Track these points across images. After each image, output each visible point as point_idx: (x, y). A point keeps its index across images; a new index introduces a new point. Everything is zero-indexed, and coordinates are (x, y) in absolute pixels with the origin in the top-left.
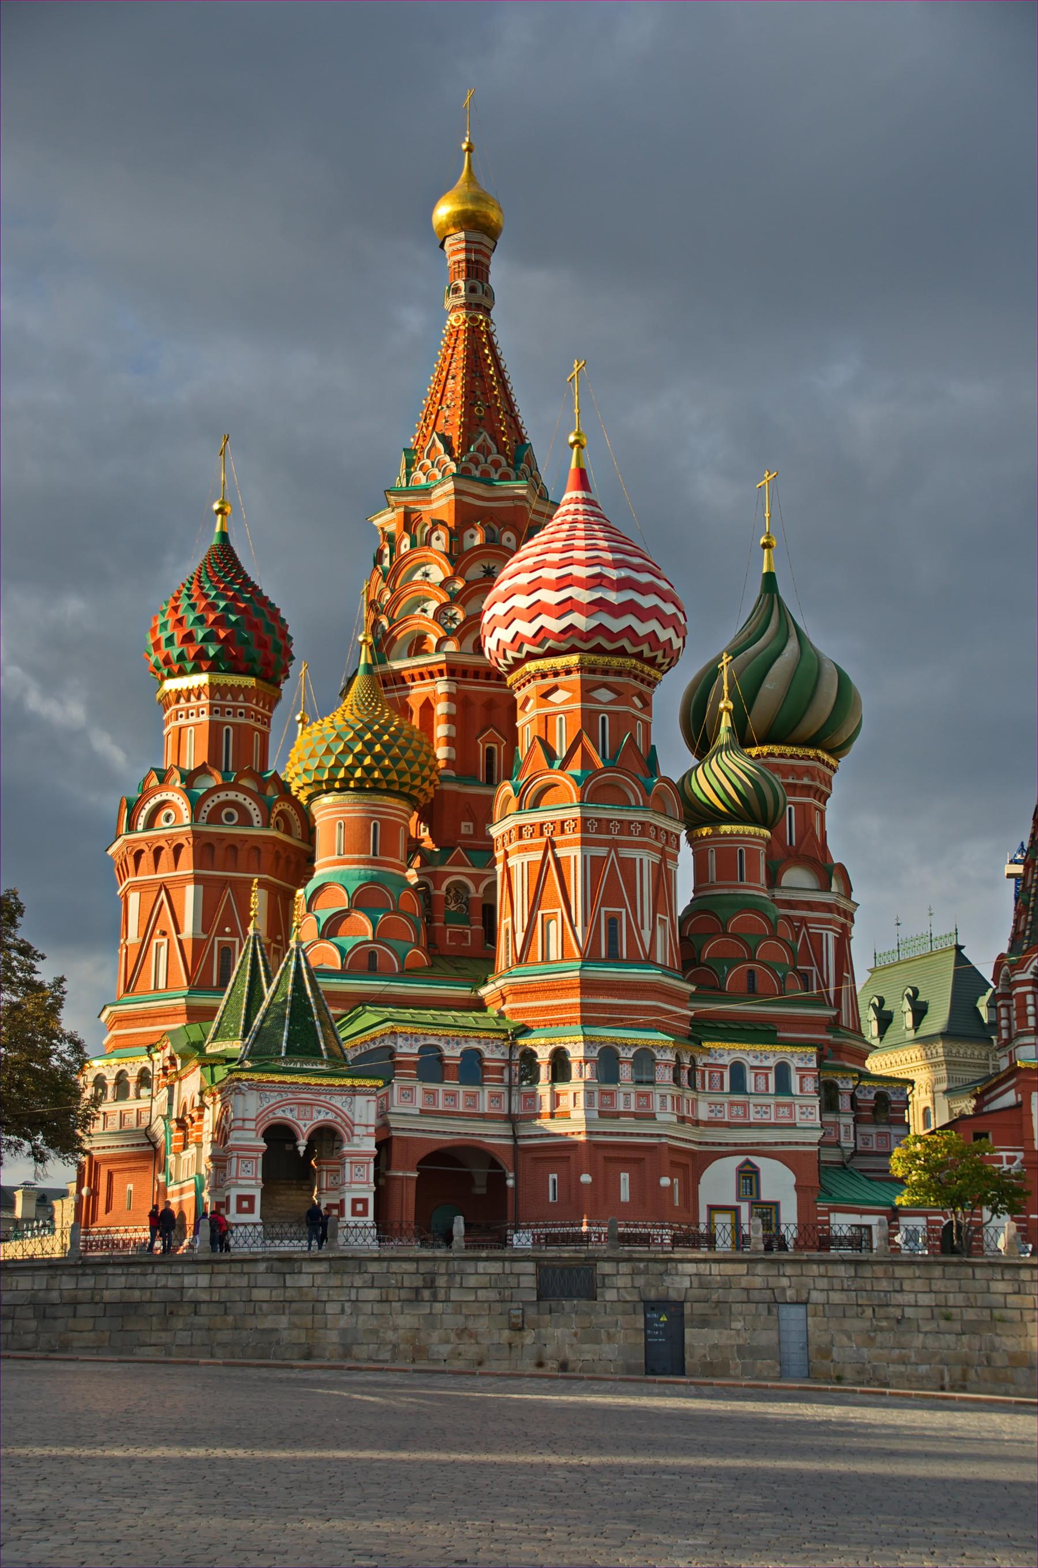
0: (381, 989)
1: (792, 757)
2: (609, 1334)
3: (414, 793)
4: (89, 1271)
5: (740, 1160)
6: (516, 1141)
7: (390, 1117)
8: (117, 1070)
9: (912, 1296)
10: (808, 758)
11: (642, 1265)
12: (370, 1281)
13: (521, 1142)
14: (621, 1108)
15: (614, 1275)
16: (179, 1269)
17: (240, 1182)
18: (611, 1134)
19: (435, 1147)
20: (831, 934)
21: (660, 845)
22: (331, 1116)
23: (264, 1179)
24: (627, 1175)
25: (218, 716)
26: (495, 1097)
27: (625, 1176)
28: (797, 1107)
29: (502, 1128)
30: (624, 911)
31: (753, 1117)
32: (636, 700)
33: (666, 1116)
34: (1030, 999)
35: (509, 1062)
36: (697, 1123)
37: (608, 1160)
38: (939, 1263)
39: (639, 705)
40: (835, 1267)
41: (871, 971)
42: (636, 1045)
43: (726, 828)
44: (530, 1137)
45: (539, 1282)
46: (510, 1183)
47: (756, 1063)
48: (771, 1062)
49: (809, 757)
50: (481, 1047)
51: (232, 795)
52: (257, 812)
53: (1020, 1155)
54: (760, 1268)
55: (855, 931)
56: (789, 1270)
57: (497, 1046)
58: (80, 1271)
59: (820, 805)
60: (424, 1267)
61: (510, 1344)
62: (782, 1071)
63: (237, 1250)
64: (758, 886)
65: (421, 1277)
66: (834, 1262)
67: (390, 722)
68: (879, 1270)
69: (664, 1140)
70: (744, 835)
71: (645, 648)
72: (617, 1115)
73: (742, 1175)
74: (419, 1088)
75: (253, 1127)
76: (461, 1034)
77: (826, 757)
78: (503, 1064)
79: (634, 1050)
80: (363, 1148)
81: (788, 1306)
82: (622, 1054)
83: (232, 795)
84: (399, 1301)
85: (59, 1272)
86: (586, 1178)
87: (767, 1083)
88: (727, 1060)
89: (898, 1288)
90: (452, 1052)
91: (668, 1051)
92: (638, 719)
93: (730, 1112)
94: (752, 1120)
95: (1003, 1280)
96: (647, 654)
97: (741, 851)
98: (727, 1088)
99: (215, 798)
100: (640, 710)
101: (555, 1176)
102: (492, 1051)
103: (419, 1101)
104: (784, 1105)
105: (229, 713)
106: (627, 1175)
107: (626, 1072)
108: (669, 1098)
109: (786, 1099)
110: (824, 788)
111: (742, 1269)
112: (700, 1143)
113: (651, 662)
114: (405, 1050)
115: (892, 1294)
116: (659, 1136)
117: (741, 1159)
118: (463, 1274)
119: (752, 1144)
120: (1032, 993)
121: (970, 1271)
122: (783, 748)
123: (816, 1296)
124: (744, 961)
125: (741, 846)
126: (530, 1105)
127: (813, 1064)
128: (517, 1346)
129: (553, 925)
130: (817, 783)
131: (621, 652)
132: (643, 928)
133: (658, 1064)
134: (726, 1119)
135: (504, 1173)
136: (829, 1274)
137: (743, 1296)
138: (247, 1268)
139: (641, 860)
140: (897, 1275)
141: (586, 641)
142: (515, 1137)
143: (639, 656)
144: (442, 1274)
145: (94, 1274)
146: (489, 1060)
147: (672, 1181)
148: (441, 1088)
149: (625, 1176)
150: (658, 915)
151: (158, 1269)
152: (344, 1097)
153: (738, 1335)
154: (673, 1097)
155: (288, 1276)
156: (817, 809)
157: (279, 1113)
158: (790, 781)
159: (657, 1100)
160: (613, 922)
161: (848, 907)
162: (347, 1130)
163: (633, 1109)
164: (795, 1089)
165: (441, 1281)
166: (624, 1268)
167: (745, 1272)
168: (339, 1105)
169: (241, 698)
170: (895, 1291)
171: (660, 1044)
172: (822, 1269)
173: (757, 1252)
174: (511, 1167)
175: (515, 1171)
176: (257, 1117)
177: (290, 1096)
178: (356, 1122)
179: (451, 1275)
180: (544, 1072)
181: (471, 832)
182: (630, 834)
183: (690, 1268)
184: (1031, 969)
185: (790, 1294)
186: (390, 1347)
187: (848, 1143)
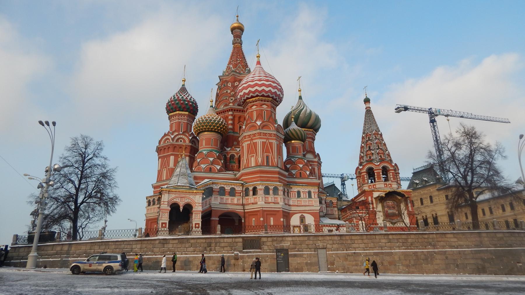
0: (212, 175)
2: (265, 260)
3: (223, 133)
4: (104, 244)
5: (300, 214)
6: (244, 211)
7: (211, 204)
8: (153, 198)
9: (358, 245)
10: (310, 131)
13: (245, 211)
14: (270, 201)
16: (131, 243)
17: (162, 219)
18: (268, 208)
19: (223, 212)
20: (317, 168)
22: (189, 201)
23: (170, 218)
24: (272, 218)
26: (238, 200)
27: (272, 219)
29: (241, 207)
33: (281, 203)
34: (365, 176)
35: (242, 191)
36: (289, 205)
37: (267, 214)
40: (334, 237)
43: (293, 141)
44: (248, 209)
45: (243, 245)
46: (243, 221)
48: (307, 190)
51: (181, 136)
56: (320, 238)
57: (239, 187)
58: (101, 244)
60: (208, 241)
61: (234, 264)
62: (310, 193)
66: (334, 235)
69: (281, 209)
71: (274, 96)
72: (269, 203)
74: (219, 197)
76: (230, 184)
77: (314, 131)
78: (241, 192)
79: (273, 187)
80: (199, 209)
81: (320, 249)
83: (181, 136)
84: (200, 251)
85: (95, 244)
86: (262, 219)
87: (306, 195)
88: (296, 190)
89: (353, 243)
90: (228, 188)
91: (282, 187)
92: (273, 112)
93: (297, 202)
94: (303, 205)
95: (384, 239)
96: (275, 97)
99: (177, 137)
101: (254, 219)
103: (219, 200)
104: (310, 201)
105: (182, 120)
108: (282, 198)
111: (306, 238)
115: (352, 244)
116: (280, 208)
117: (300, 214)
118: (220, 242)
119: (303, 210)
120: (366, 174)
121: (374, 236)
122: (305, 129)
123: (329, 246)
125: (297, 145)
126: (248, 201)
128: (236, 265)
129: (253, 158)
131: (268, 96)
133: (279, 190)
135: (241, 219)
136: (332, 239)
137: (307, 247)
138: (152, 242)
139: (274, 143)
140: (353, 238)
142: (244, 210)
144: (213, 243)
145: (105, 245)
146: (237, 190)
147: (284, 220)
148: (225, 197)
149: (272, 219)
151: (125, 243)
152: (193, 196)
153: (306, 259)
154: (283, 198)
155: (165, 245)
156: (312, 142)
157: (175, 200)
159: (279, 199)
160: (267, 157)
163: (273, 201)
164: (313, 197)
165: (213, 245)
166: (270, 239)
167: (307, 239)
168: (192, 198)
170: (353, 244)
171: (280, 185)
172: (330, 238)
174: (243, 217)
176: (168, 201)
177: (178, 195)
178: (196, 202)
179: (216, 243)
180: (251, 193)
181: (236, 144)
182: (271, 136)
183: (290, 239)
184: (365, 169)
185: (321, 246)
186: (196, 266)
187: (325, 211)
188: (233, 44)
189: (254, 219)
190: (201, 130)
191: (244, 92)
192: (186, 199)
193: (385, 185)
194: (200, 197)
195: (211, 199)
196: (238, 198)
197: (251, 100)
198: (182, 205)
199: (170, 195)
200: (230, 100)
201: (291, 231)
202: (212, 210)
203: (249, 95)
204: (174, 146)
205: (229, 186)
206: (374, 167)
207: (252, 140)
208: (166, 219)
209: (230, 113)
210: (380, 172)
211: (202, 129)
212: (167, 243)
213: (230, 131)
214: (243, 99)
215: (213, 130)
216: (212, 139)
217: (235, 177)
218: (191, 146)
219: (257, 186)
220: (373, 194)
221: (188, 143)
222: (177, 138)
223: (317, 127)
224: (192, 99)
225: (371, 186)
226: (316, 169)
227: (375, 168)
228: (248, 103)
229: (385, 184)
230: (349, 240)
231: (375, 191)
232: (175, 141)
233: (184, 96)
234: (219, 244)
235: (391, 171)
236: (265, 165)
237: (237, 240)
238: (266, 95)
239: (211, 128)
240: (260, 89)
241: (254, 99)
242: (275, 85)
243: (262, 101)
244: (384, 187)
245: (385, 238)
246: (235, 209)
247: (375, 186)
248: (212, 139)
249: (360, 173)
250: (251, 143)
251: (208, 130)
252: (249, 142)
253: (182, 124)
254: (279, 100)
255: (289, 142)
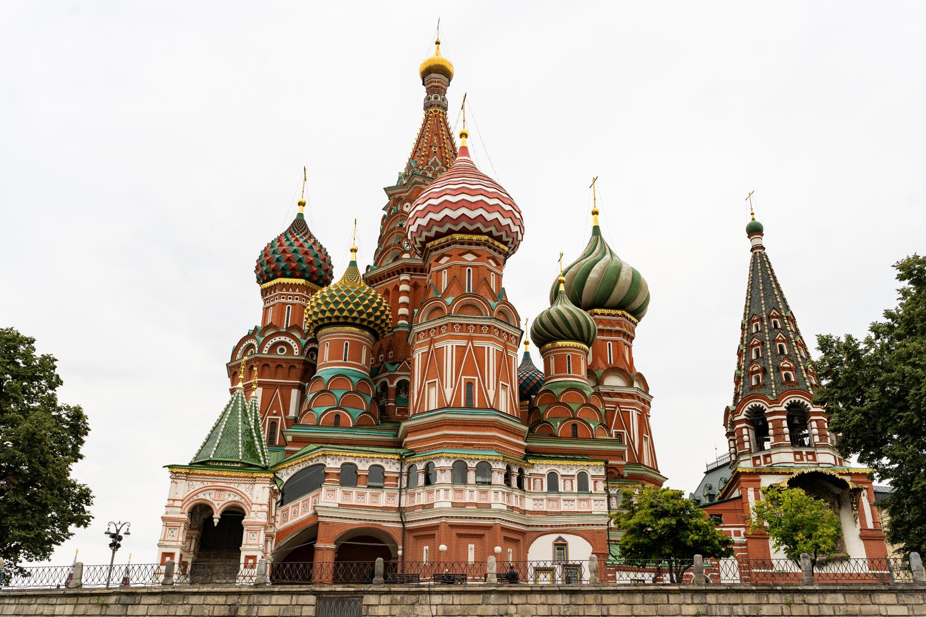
1: (608, 315)
3: (376, 329)
5: (556, 536)
6: (404, 525)
11: (399, 597)
12: (189, 611)
13: (408, 526)
14: (468, 500)
15: (377, 605)
19: (348, 528)
20: (634, 411)
21: (503, 341)
22: (237, 498)
24: (473, 546)
25: (284, 300)
26: (390, 496)
28: (592, 500)
30: (476, 378)
31: (563, 507)
32: (491, 261)
34: (745, 431)
35: (401, 473)
37: (459, 535)
38: (639, 591)
39: (494, 265)
41: (707, 473)
42: (478, 459)
43: (560, 343)
44: (412, 522)
46: (400, 552)
47: (565, 473)
48: (574, 472)
49: (618, 315)
50: (383, 464)
51: (283, 339)
52: (297, 347)
53: (742, 530)
54: (493, 598)
55: (652, 412)
56: (516, 599)
59: (628, 343)
60: (231, 600)
63: (86, 587)
64: (579, 376)
65: (228, 607)
67: (367, 294)
68: (590, 599)
69: (497, 522)
70: (570, 347)
72: (466, 504)
73: (556, 547)
74: (339, 491)
75: (180, 505)
77: (629, 316)
78: (397, 475)
79: (477, 462)
80: (258, 520)
82: (469, 465)
83: (283, 339)
88: (545, 471)
91: (500, 463)
94: (562, 510)
95: (693, 604)
96: (495, 233)
97: (569, 357)
98: (545, 489)
100: (495, 267)
102: (390, 467)
105: (290, 298)
106: (473, 546)
107: (471, 477)
108: (500, 493)
109: (585, 496)
110: (629, 333)
111: (478, 599)
112: (528, 526)
113: (499, 239)
114: (332, 466)
116: (494, 518)
117: (556, 536)
121: (665, 596)
124: (570, 419)
125: (568, 354)
127: (603, 473)
130: (625, 330)
132: (489, 388)
134: (545, 510)
136: (549, 602)
139: (488, 348)
141: (456, 225)
143: (490, 234)
146: (388, 472)
148: (354, 491)
149: (471, 546)
150: (501, 382)
152: (248, 485)
154: (503, 493)
156: (625, 344)
157: (201, 496)
158: (608, 328)
160: (470, 384)
161: (646, 397)
162: (249, 508)
163: (475, 501)
164: (591, 488)
166: (385, 599)
168: (244, 491)
169: (297, 290)
171: (494, 458)
173: (491, 585)
175: (403, 545)
177: (210, 484)
178: (254, 502)
180: (421, 479)
182: (481, 332)
184: (744, 413)
188: (426, 108)
189: (426, 548)
190: (320, 323)
191: (419, 225)
192: (230, 493)
193: (798, 457)
194: (264, 488)
195: (318, 495)
196: (390, 491)
197: (437, 242)
198: (218, 507)
199: (191, 483)
200: (405, 245)
201: (529, 577)
202: (320, 524)
203: (429, 231)
204: (289, 365)
205: (367, 462)
206: (765, 407)
207: (432, 342)
208: (174, 544)
209: (404, 277)
210: (782, 420)
211: (322, 319)
212: (135, 604)
213: (400, 322)
214: (420, 242)
215: (349, 321)
216: (347, 344)
217: (396, 438)
218: (305, 362)
219: (434, 462)
220: (759, 481)
221: (297, 354)
222: (271, 343)
223: (637, 304)
224: (316, 249)
225: (759, 458)
226: (634, 416)
227: (767, 409)
228: (431, 251)
229: (795, 453)
230: (594, 606)
231: (764, 473)
232: (267, 349)
233: (306, 241)
234: (258, 609)
235: (812, 418)
236: (463, 406)
237: (303, 599)
238: (471, 228)
239: (353, 318)
240: (455, 215)
241: (443, 240)
242: (496, 201)
243: (462, 244)
244: (793, 460)
245: (695, 602)
246: (379, 521)
247: (768, 459)
248: (347, 344)
249: (733, 424)
250: (429, 349)
251: (336, 321)
252: (425, 349)
253: (289, 308)
254: (511, 240)
255: (550, 345)
